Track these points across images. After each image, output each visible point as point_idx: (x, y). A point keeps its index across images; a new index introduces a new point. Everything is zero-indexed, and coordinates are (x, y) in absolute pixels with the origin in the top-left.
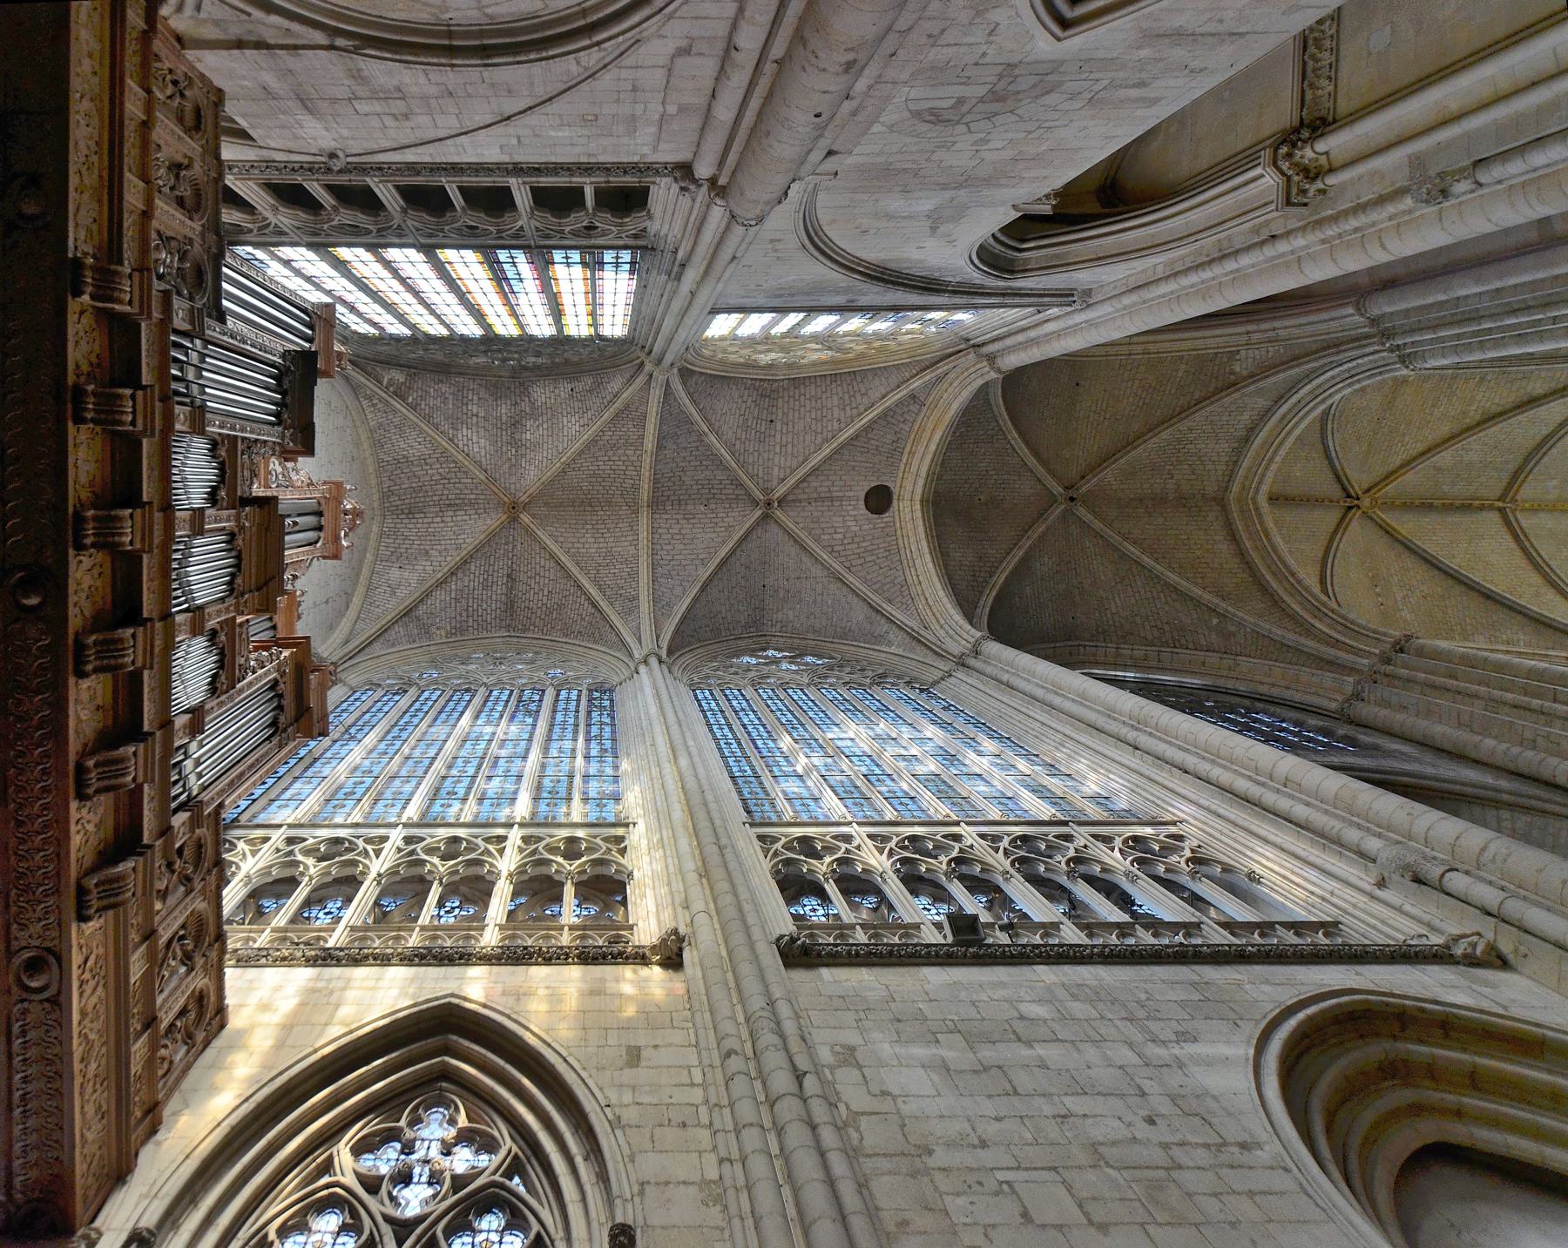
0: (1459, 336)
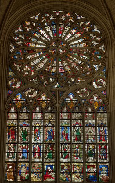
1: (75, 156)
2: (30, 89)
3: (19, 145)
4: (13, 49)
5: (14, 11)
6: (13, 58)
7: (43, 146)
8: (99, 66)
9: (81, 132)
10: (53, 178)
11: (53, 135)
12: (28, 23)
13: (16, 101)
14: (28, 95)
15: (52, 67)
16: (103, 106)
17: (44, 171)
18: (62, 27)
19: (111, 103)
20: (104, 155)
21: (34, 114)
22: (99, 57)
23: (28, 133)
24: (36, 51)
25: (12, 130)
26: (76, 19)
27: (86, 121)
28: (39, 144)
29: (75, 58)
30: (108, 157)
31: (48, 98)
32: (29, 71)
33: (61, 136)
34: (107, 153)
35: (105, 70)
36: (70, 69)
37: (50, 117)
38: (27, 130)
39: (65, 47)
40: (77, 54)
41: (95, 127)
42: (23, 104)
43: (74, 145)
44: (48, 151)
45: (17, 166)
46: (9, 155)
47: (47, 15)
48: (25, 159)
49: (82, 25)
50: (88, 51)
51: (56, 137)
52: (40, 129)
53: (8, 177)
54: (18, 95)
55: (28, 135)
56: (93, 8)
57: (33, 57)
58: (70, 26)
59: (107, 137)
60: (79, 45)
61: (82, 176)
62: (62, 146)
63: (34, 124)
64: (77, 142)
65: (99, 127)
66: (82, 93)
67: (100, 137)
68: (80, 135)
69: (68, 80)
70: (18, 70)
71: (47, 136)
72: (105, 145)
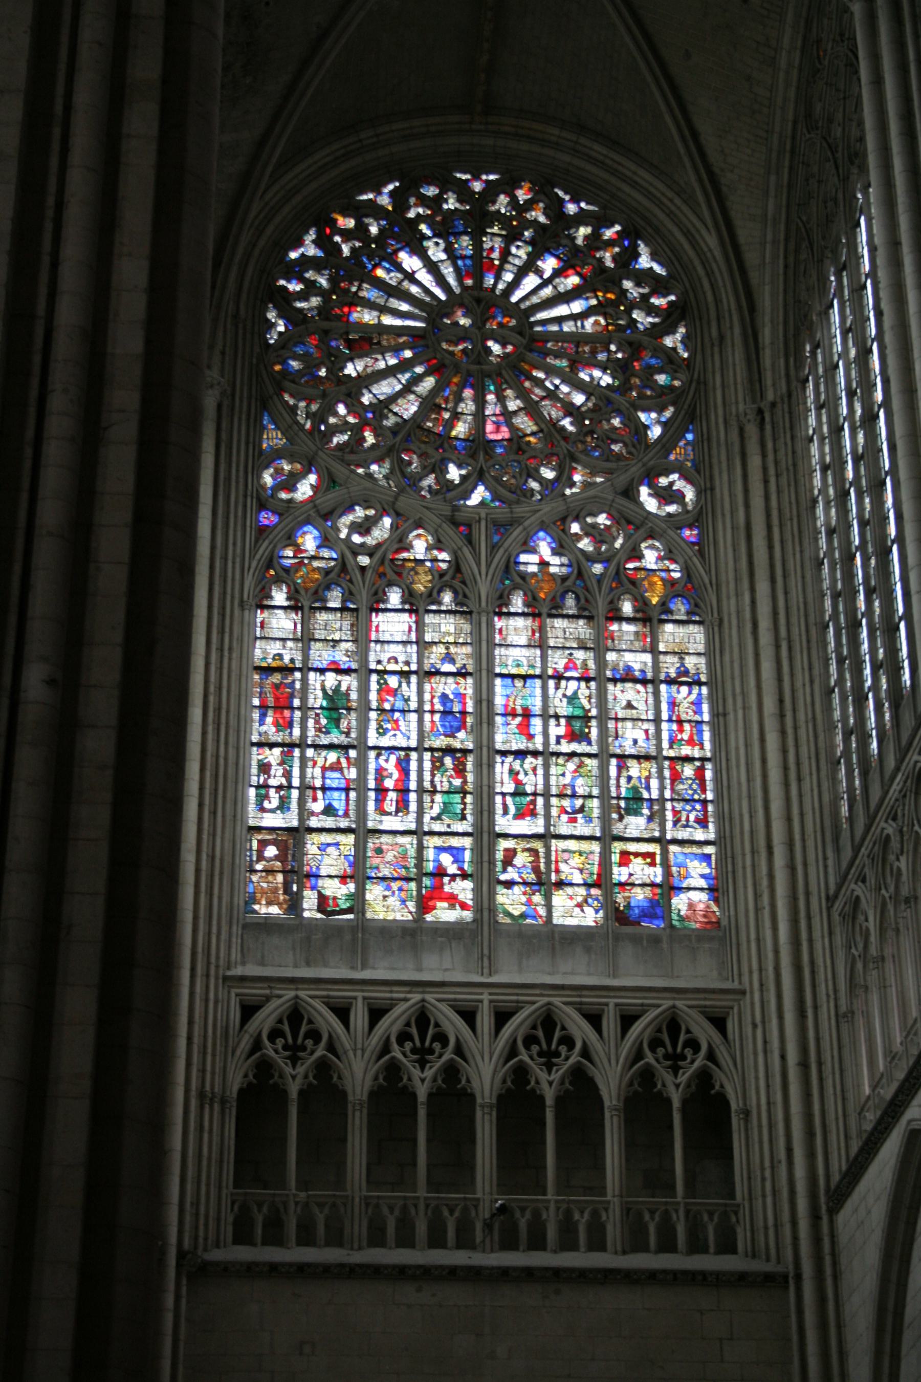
1: (563, 811)
2: (357, 508)
3: (310, 752)
4: (281, 328)
6: (278, 368)
7: (420, 761)
8: (663, 419)
9: (589, 702)
10: (464, 906)
11: (464, 713)
12: (347, 220)
13: (295, 557)
14: (349, 535)
15: (456, 416)
16: (686, 593)
17: (426, 874)
18: (498, 243)
19: (723, 578)
20: (694, 809)
21: (377, 616)
22: (661, 379)
23: (349, 701)
24: (384, 343)
25: (276, 687)
27: (611, 657)
28: (402, 753)
29: (557, 382)
30: (711, 819)
31: (440, 550)
32: (351, 431)
33: (499, 720)
34: (704, 802)
35: (690, 437)
36: (535, 428)
37: (449, 634)
38: (344, 688)
39: (512, 329)
40: (565, 363)
41: (651, 682)
42: (327, 572)
43: (561, 760)
44: (441, 782)
45: (300, 845)
46: (262, 798)
47: (431, 191)
48: (337, 816)
49: (586, 238)
50: (616, 352)
51: (479, 722)
52: (404, 685)
53: (258, 895)
54: (305, 533)
55: (349, 709)
56: (633, 167)
57: (369, 370)
58: (531, 242)
59: (706, 728)
60: (571, 323)
61: (597, 899)
62: (503, 762)
63: (379, 662)
64: (575, 747)
65: (670, 682)
66: (591, 531)
67: (675, 727)
68: (586, 718)
69: (529, 476)
70: (302, 422)
71: (437, 717)
72: (698, 764)
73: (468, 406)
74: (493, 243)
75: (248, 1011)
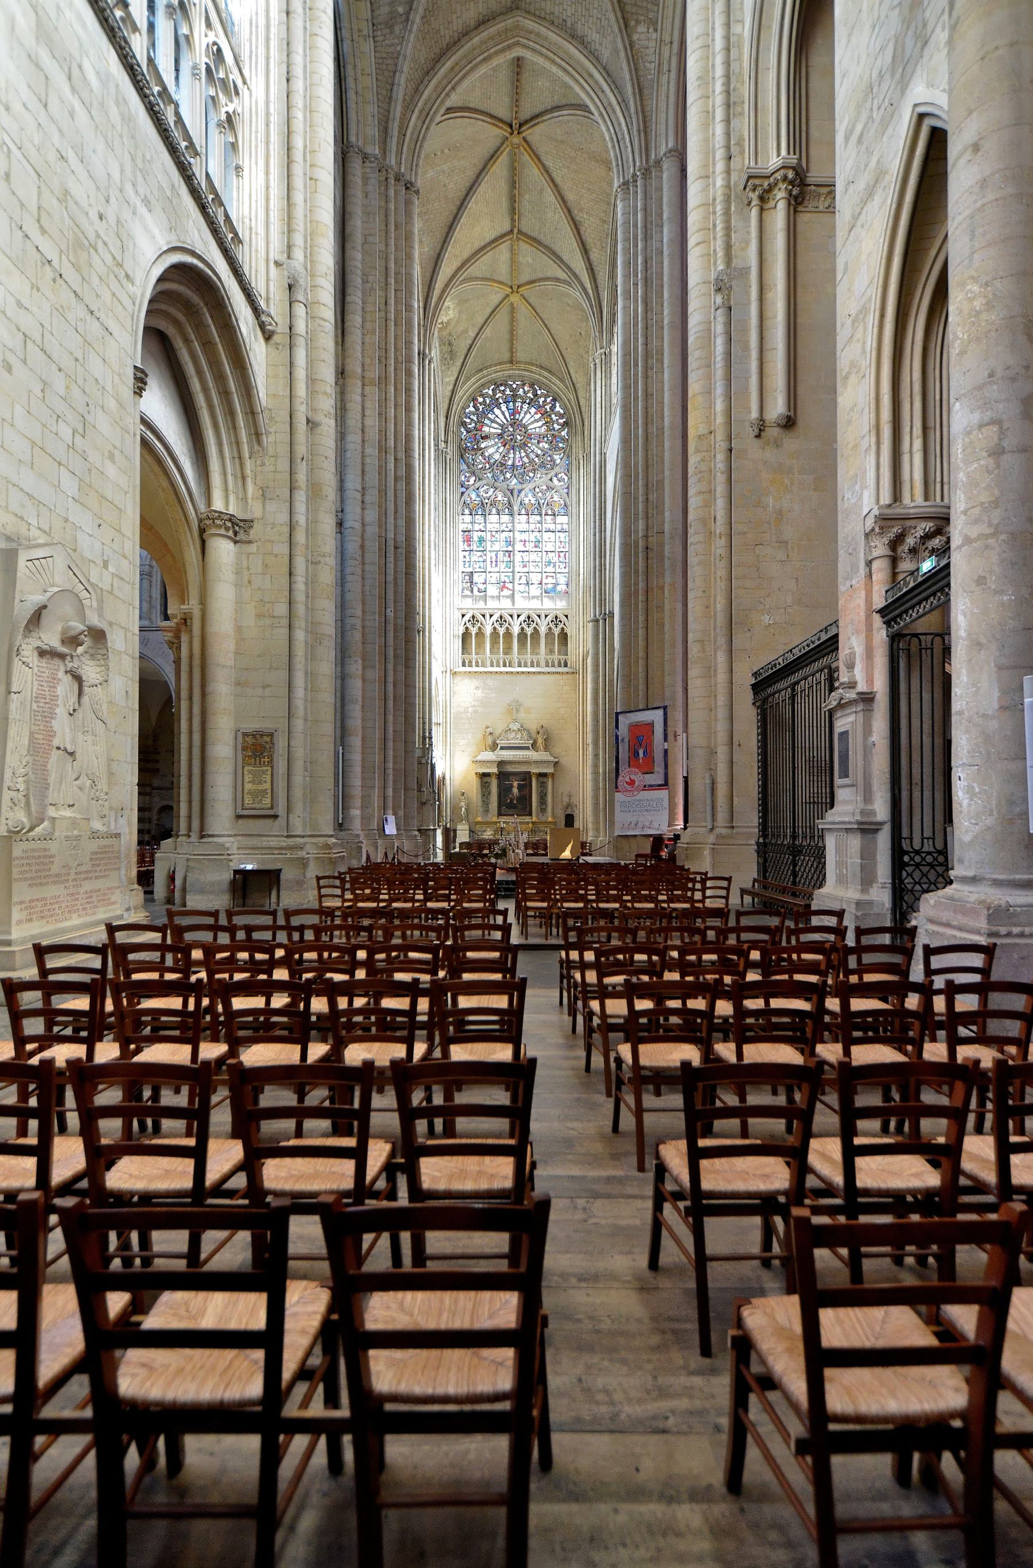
0: (636, 226)
5: (464, 383)
22: (561, 445)
26: (535, 395)
47: (502, 388)
73: (511, 455)
74: (519, 404)
75: (463, 616)
